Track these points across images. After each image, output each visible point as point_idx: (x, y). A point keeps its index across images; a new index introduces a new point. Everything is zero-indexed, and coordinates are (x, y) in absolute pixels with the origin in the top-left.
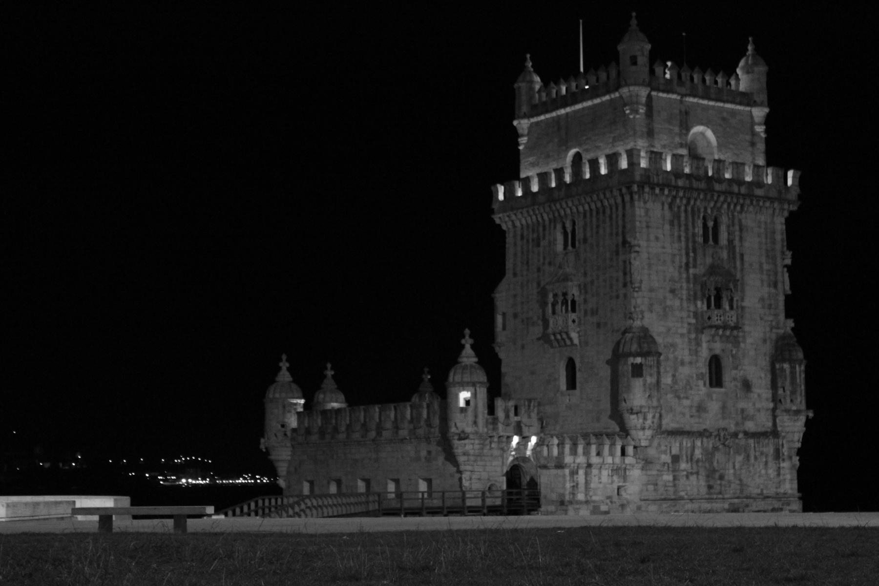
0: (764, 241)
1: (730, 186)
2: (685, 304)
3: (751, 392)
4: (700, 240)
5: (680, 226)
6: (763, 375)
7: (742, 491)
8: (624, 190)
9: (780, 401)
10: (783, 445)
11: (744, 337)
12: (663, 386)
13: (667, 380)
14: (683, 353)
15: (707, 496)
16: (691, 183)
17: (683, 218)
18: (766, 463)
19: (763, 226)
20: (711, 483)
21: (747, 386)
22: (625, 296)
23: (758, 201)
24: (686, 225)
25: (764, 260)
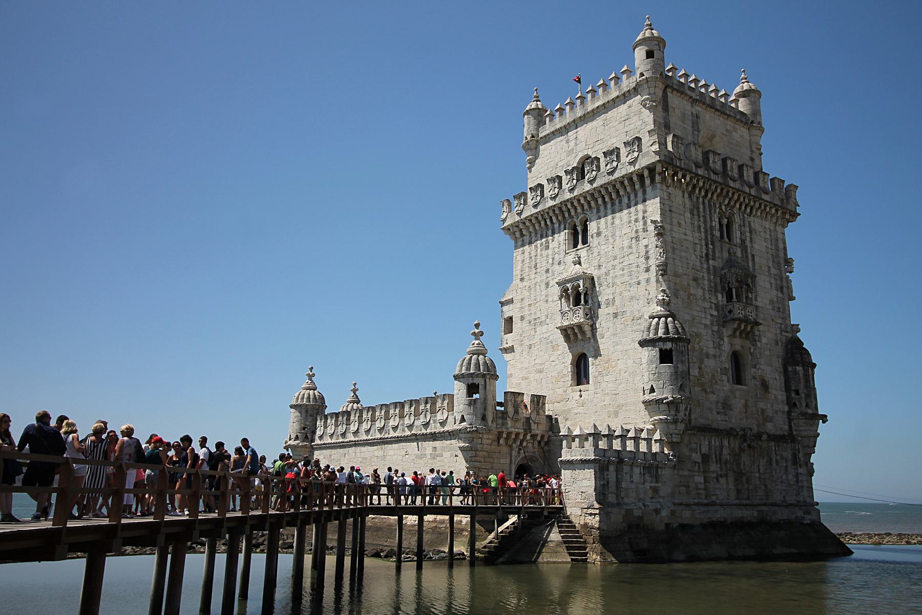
1: (742, 186)
2: (707, 296)
4: (718, 234)
8: (646, 173)
9: (795, 404)
11: (760, 336)
13: (695, 372)
14: (707, 343)
15: (737, 502)
16: (709, 174)
17: (701, 210)
20: (740, 487)
21: (765, 386)
22: (648, 281)
23: (766, 206)
24: (704, 216)
25: (771, 264)
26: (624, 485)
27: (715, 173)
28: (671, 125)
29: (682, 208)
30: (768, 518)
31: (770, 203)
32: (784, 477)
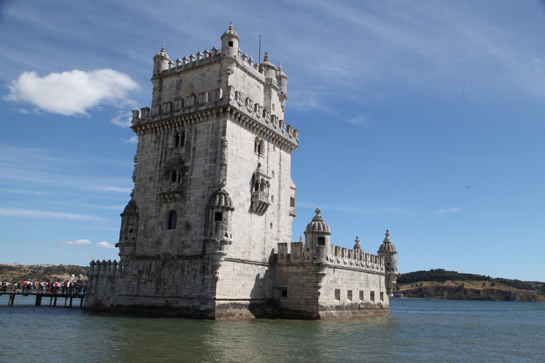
0: (210, 136)
1: (184, 111)
2: (156, 185)
3: (190, 230)
5: (159, 142)
6: (200, 219)
7: (177, 293)
10: (208, 263)
11: (190, 197)
12: (139, 231)
18: (195, 275)
19: (211, 127)
20: (159, 287)
21: (188, 226)
24: (163, 141)
25: (208, 147)
26: (98, 286)
27: (165, 115)
28: (162, 97)
29: (150, 143)
30: (172, 305)
31: (203, 110)
32: (192, 281)
